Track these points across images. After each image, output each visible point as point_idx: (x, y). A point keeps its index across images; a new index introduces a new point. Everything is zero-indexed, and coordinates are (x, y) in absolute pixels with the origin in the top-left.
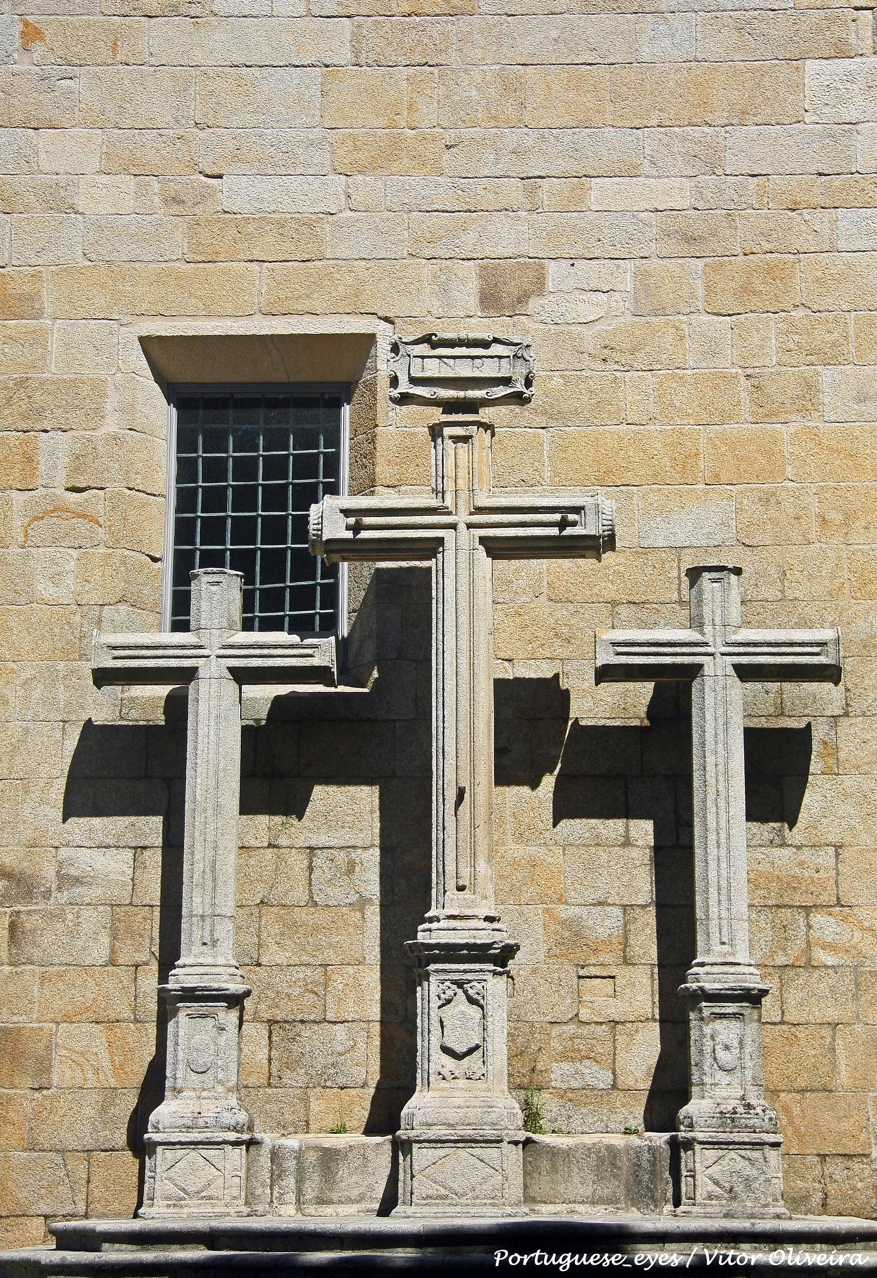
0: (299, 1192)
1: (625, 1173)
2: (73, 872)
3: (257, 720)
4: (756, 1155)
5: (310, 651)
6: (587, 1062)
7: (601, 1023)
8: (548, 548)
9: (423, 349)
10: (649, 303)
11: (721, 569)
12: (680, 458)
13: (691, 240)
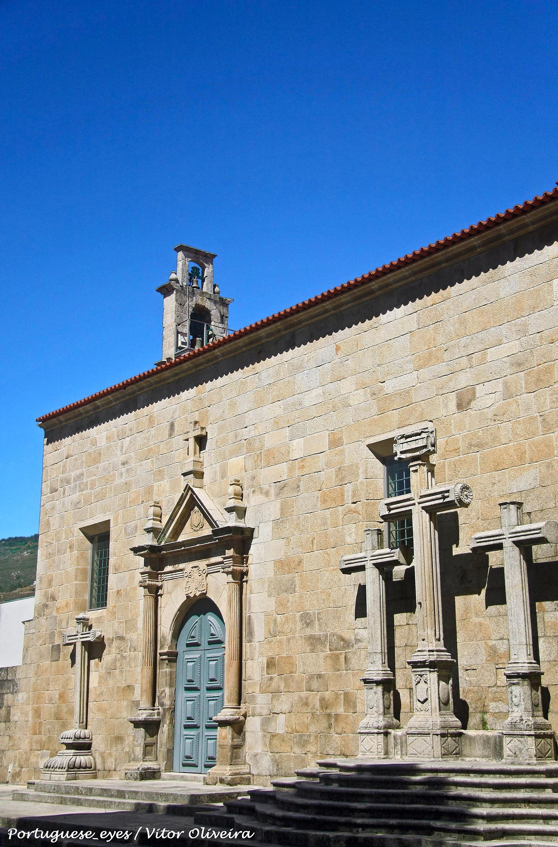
0: (402, 752)
1: (492, 746)
2: (359, 638)
3: (402, 578)
4: (522, 739)
5: (393, 555)
6: (500, 702)
7: (504, 687)
8: (444, 507)
9: (403, 440)
10: (508, 394)
11: (505, 504)
12: (520, 455)
13: (519, 365)
